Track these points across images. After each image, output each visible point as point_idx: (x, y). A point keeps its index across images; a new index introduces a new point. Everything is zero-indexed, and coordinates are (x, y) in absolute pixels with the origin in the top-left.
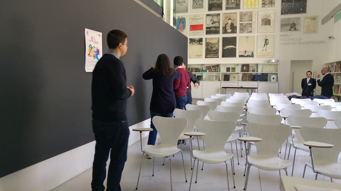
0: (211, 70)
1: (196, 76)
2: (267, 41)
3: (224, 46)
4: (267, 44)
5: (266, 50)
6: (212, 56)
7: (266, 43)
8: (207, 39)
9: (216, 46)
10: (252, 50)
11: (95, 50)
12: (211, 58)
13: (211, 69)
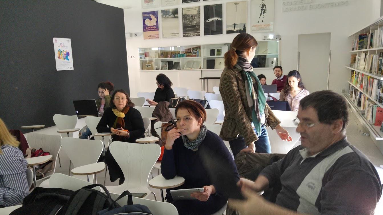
0: (190, 54)
1: (173, 63)
2: (264, 8)
3: (206, 18)
4: (264, 12)
5: (263, 22)
6: (193, 34)
7: (263, 11)
8: (184, 9)
9: (196, 19)
10: (244, 23)
11: (65, 53)
12: (190, 36)
13: (191, 52)
